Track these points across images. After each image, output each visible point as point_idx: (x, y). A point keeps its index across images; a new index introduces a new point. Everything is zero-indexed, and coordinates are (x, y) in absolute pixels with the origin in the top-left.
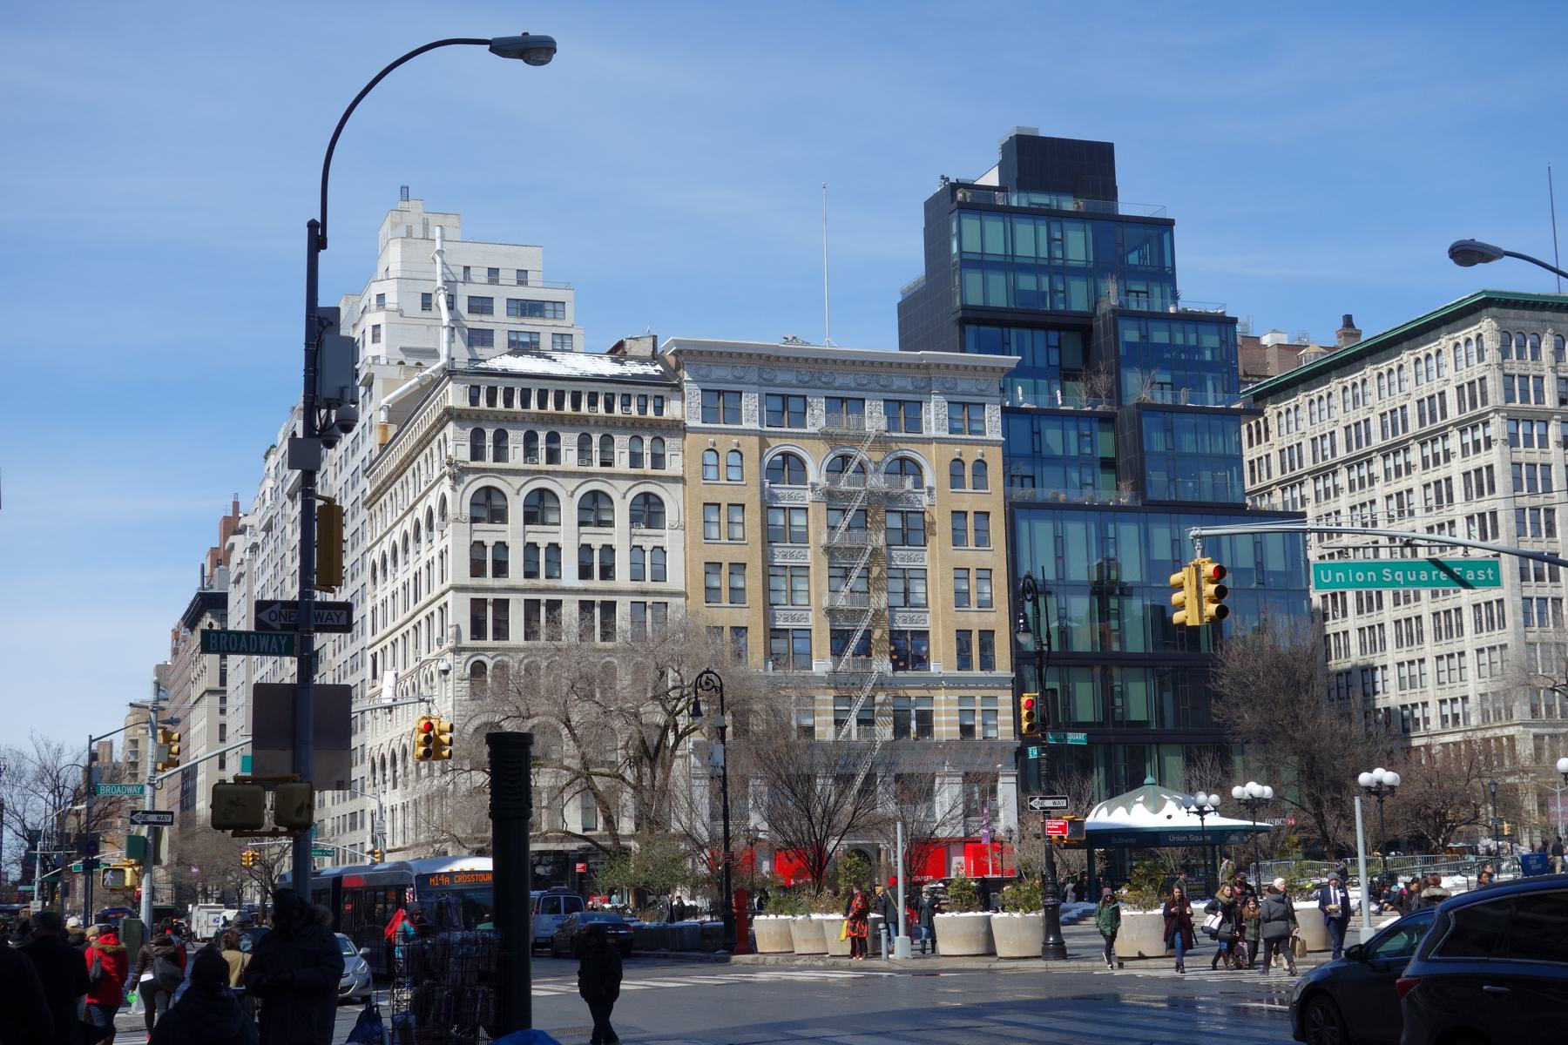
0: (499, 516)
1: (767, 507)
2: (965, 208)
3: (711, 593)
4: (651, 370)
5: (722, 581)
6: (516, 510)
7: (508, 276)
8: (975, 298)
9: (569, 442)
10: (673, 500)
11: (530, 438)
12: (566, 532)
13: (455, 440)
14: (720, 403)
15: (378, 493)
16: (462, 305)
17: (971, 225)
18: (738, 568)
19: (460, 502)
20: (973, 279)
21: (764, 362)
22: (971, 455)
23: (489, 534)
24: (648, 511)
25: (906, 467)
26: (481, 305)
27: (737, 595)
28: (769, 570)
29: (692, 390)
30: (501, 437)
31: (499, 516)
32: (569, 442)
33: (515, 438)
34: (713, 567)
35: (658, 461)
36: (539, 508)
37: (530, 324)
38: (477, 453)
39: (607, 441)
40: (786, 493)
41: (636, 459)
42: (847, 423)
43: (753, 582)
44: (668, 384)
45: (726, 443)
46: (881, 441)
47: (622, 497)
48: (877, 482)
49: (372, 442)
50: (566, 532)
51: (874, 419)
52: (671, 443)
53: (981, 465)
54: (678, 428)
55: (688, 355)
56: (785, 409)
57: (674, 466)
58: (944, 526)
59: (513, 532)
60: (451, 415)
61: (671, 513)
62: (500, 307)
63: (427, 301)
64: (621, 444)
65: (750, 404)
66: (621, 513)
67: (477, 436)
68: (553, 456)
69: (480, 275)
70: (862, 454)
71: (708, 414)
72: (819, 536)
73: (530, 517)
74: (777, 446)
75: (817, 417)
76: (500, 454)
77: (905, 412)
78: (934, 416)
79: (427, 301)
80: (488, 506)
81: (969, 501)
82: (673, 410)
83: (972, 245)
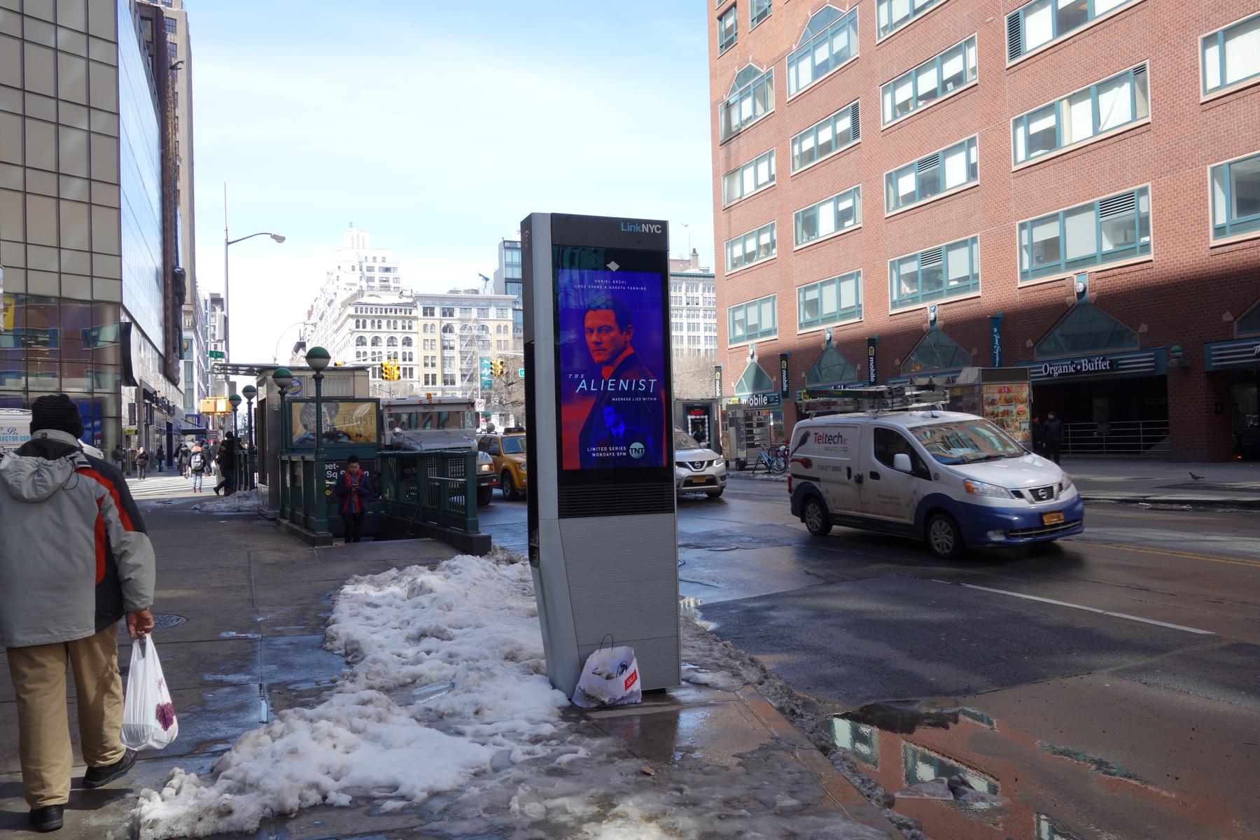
0: (364, 344)
1: (442, 340)
2: (506, 248)
3: (426, 365)
4: (410, 300)
5: (430, 363)
6: (369, 342)
7: (379, 260)
8: (510, 276)
9: (384, 322)
10: (414, 337)
11: (373, 322)
12: (383, 348)
13: (352, 322)
14: (428, 312)
15: (337, 331)
16: (364, 269)
17: (509, 253)
18: (433, 357)
19: (353, 340)
20: (509, 269)
21: (441, 298)
22: (503, 324)
23: (361, 349)
24: (407, 342)
25: (483, 328)
26: (370, 269)
27: (433, 365)
28: (443, 359)
29: (420, 309)
30: (364, 322)
31: (364, 344)
32: (384, 322)
33: (369, 322)
34: (426, 357)
35: (410, 328)
36: (375, 341)
37: (386, 274)
38: (358, 327)
39: (395, 322)
40: (448, 336)
41: (404, 327)
42: (467, 316)
43: (438, 362)
44: (413, 305)
45: (429, 322)
46: (476, 320)
47: (400, 338)
48: (475, 332)
49: (337, 312)
50: (383, 348)
51: (474, 314)
52: (414, 323)
53: (506, 327)
54: (416, 318)
55: (419, 298)
56: (448, 312)
57: (414, 329)
58: (494, 345)
59: (368, 348)
60: (350, 316)
61: (414, 343)
62: (376, 269)
63: (353, 268)
64: (399, 323)
65: (437, 311)
66: (400, 343)
67: (358, 321)
68: (379, 327)
69: (370, 259)
70: (470, 324)
71: (425, 314)
72: (457, 348)
73: (373, 344)
74: (445, 323)
75: (457, 313)
76: (364, 327)
77: (483, 311)
78: (492, 312)
79: (353, 268)
80: (361, 341)
81: (502, 337)
82: (414, 313)
83: (509, 260)
